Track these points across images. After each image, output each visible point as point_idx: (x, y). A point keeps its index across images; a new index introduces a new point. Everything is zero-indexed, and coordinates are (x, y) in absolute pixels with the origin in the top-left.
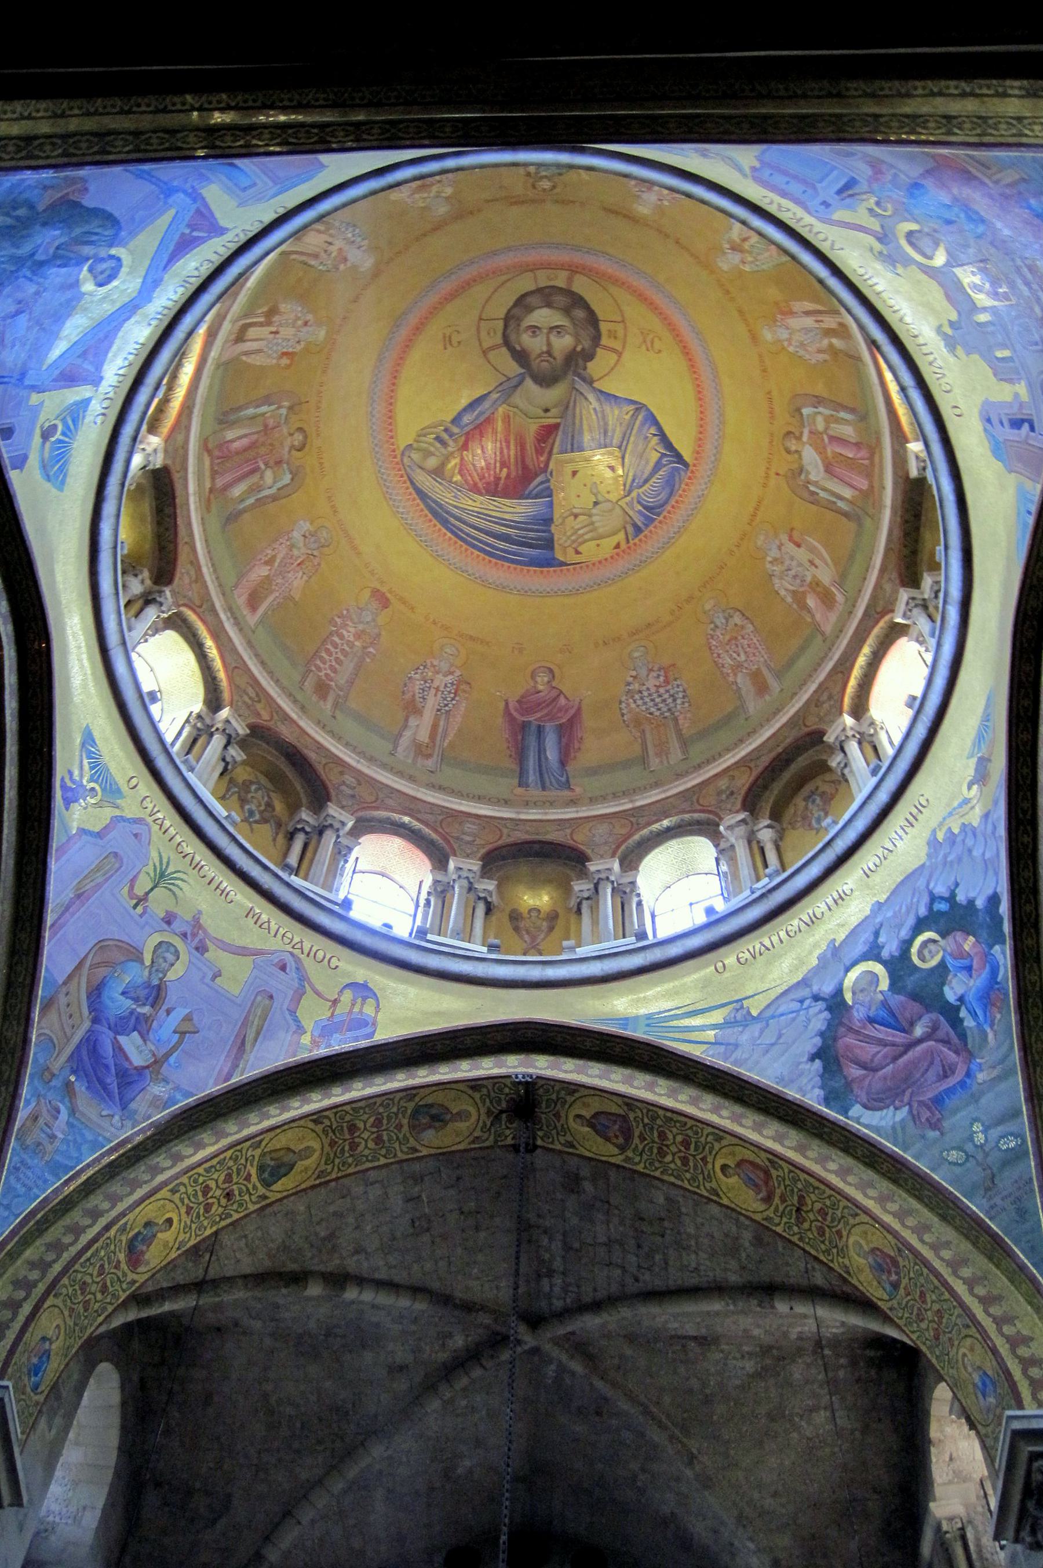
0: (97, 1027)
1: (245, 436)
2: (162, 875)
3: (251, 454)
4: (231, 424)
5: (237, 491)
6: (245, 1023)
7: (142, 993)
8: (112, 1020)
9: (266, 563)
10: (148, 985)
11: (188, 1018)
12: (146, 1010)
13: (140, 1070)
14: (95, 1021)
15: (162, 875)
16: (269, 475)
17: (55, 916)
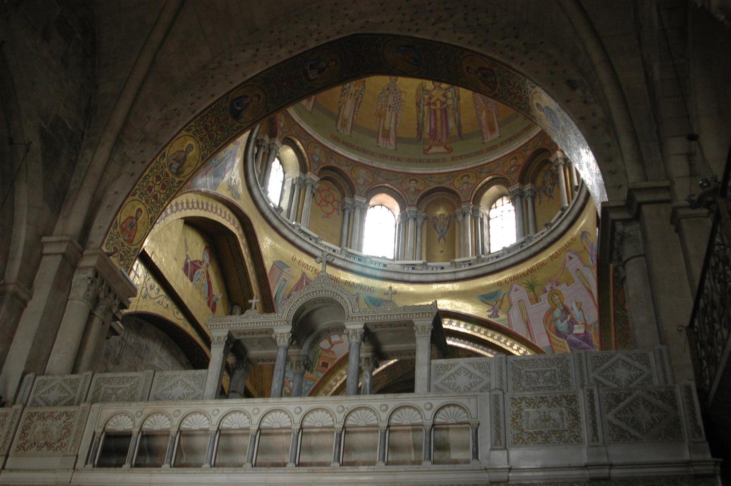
0: (568, 338)
1: (430, 118)
2: (530, 285)
3: (439, 113)
4: (423, 126)
5: (451, 124)
6: (584, 285)
7: (564, 315)
8: (568, 332)
9: (482, 111)
10: (562, 311)
11: (577, 303)
12: (569, 317)
13: (585, 332)
14: (566, 338)
15: (530, 285)
16: (450, 102)
17: (529, 336)
